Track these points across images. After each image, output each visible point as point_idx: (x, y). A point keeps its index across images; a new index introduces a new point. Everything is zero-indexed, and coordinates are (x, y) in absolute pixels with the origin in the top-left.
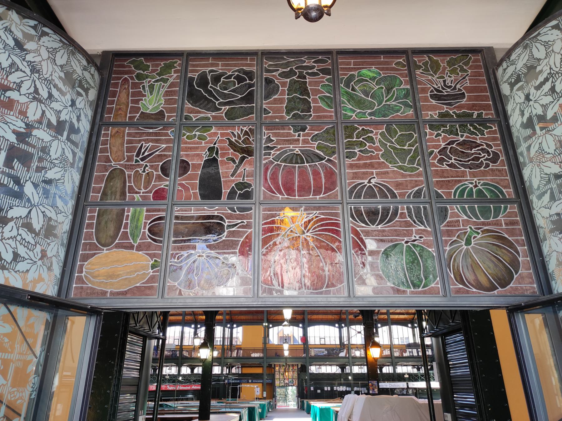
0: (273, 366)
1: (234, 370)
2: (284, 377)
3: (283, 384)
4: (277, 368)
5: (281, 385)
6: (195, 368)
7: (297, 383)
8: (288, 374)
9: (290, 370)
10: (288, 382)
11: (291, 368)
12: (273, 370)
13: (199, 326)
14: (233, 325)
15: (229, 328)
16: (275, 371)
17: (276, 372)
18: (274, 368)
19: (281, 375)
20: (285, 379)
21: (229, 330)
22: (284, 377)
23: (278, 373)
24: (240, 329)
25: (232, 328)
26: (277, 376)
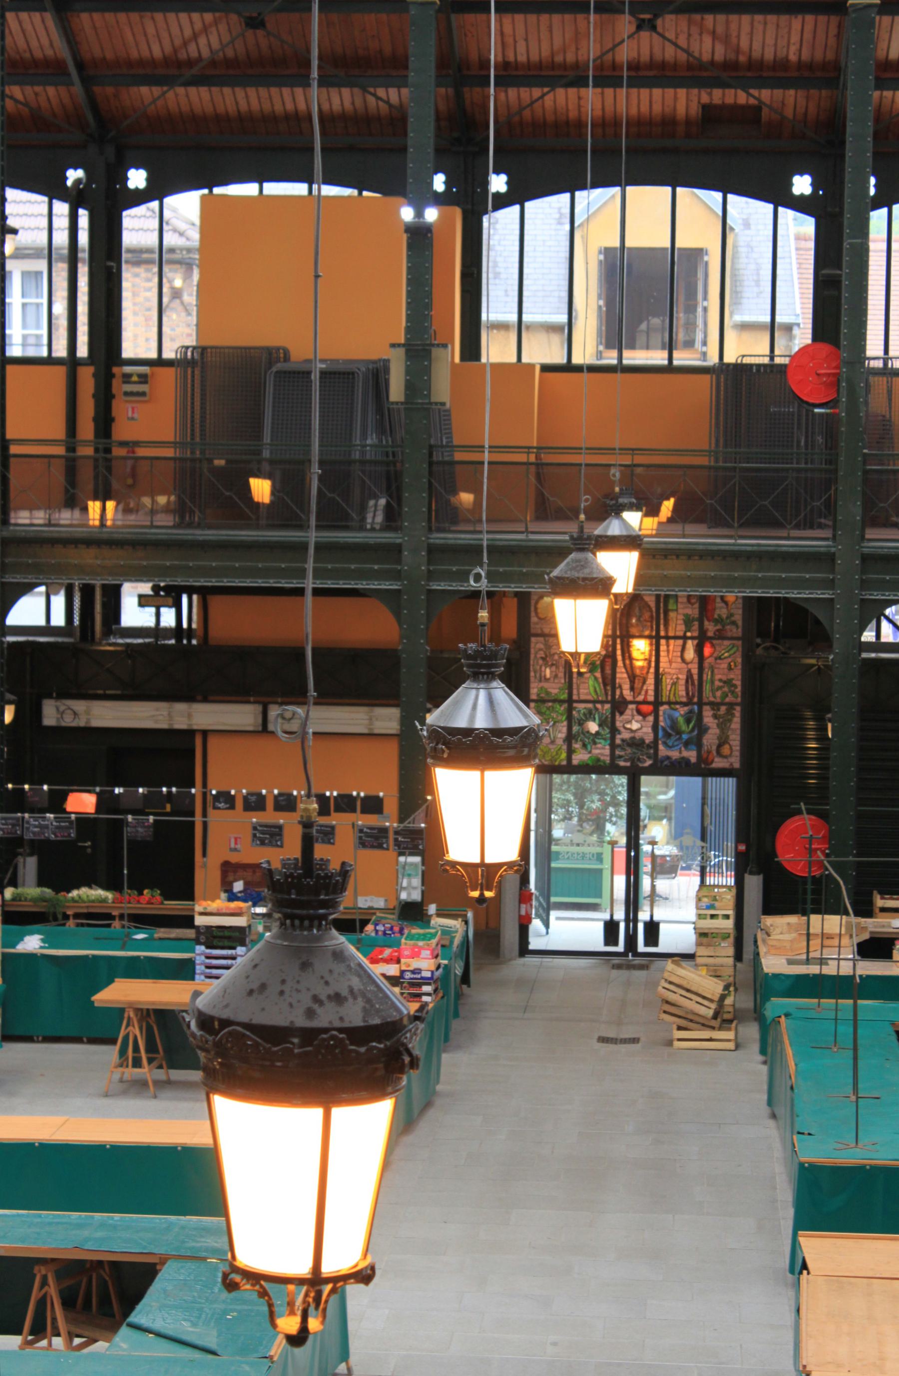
2: (609, 682)
3: (602, 751)
5: (580, 757)
7: (735, 739)
9: (677, 626)
10: (647, 733)
20: (619, 706)
21: (84, 218)
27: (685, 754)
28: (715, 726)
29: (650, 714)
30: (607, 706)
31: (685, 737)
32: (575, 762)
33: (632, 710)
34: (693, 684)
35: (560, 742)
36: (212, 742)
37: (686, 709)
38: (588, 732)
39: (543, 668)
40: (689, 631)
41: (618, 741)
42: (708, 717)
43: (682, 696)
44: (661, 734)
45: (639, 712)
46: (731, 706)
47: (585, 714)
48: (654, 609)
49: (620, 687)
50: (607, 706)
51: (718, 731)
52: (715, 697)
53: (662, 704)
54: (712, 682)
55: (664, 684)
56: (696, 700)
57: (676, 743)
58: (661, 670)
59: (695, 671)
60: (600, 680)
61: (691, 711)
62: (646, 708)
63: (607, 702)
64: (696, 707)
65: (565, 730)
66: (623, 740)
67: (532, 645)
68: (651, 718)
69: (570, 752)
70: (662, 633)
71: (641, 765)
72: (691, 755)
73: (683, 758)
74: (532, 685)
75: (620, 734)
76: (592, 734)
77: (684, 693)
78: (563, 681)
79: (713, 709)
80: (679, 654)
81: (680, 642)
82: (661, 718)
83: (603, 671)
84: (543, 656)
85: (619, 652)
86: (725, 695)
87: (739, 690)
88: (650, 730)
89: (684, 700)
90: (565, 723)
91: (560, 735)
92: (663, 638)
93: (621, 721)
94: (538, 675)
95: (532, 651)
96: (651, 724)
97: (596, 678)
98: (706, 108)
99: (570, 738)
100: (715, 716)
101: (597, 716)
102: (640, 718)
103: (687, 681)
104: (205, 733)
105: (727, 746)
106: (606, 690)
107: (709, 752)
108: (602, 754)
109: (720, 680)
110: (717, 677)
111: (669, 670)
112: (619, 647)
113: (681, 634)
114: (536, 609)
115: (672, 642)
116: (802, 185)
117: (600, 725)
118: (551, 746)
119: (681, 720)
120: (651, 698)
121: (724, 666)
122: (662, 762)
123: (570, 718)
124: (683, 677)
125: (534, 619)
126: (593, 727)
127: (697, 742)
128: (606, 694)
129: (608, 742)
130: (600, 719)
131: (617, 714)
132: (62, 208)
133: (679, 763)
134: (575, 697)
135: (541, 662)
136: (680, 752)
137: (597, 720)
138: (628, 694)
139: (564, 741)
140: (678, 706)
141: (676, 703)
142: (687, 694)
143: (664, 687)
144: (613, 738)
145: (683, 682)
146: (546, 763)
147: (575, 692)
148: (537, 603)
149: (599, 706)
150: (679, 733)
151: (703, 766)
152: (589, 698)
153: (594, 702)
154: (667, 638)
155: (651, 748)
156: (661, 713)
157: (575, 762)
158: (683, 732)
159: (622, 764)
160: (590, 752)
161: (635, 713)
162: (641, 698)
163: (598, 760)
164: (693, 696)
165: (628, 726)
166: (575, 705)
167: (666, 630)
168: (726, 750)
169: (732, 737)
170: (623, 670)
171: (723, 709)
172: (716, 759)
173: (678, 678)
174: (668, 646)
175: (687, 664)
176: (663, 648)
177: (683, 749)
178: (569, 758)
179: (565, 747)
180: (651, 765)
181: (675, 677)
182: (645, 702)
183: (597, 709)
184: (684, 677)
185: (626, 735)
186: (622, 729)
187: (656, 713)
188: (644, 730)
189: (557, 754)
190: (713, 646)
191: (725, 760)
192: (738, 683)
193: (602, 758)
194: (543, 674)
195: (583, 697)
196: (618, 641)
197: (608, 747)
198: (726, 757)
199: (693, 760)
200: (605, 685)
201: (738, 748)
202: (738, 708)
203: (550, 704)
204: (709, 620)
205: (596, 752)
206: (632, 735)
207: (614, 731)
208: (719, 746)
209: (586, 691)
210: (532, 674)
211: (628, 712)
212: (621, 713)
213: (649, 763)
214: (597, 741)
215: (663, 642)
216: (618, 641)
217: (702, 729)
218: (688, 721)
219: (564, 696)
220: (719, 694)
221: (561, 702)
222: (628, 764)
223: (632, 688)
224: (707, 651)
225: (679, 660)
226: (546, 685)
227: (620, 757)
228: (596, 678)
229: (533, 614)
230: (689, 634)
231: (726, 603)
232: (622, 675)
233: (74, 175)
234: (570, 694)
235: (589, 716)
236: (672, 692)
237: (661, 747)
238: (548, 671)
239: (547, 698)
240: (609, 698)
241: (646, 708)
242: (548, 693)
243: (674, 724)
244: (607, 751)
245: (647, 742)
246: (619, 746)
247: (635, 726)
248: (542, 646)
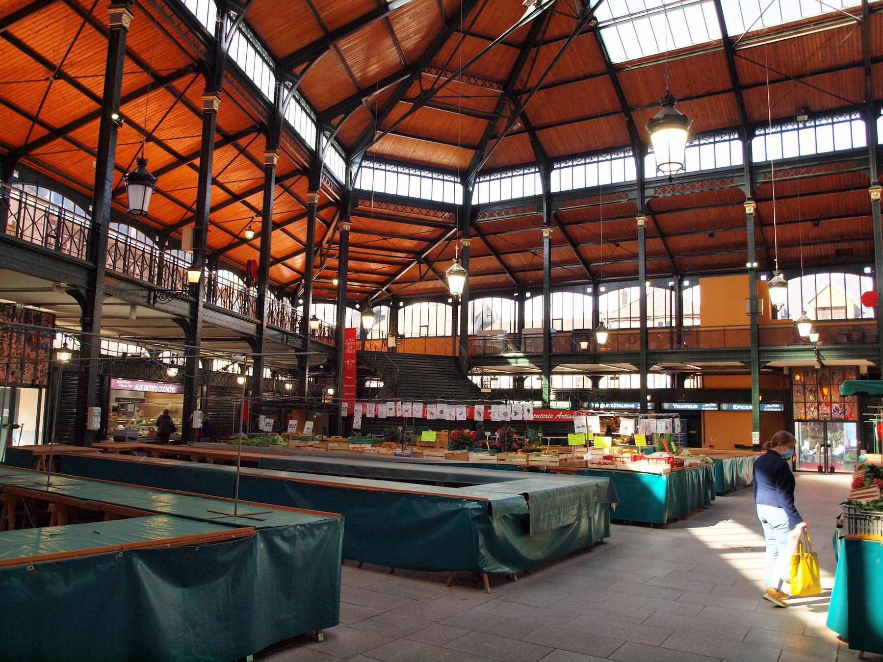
0: (786, 372)
1: (689, 384)
4: (798, 378)
6: (601, 377)
8: (830, 392)
11: (836, 378)
12: (788, 381)
13: (602, 289)
14: (680, 282)
15: (672, 288)
16: (791, 384)
17: (795, 387)
18: (790, 376)
19: (807, 394)
20: (819, 403)
21: (673, 293)
22: (816, 397)
23: (800, 388)
24: (697, 289)
25: (679, 289)
26: (797, 397)
27: (840, 416)
36: (706, 413)
42: (847, 407)
45: (826, 405)
46: (854, 403)
62: (827, 404)
68: (829, 407)
69: (806, 416)
72: (842, 416)
86: (851, 400)
98: (837, 251)
99: (805, 412)
100: (849, 406)
104: (704, 411)
116: (867, 270)
120: (829, 401)
123: (805, 407)
125: (793, 380)
126: (812, 409)
127: (844, 413)
132: (668, 291)
138: (822, 400)
150: (838, 410)
154: (833, 384)
168: (853, 415)
171: (851, 404)
176: (832, 387)
178: (806, 418)
182: (827, 402)
185: (822, 411)
187: (831, 405)
202: (856, 404)
207: (818, 410)
208: (851, 414)
217: (845, 410)
218: (841, 407)
232: (820, 395)
233: (671, 284)
235: (811, 406)
241: (827, 404)
243: (836, 407)
247: (825, 409)
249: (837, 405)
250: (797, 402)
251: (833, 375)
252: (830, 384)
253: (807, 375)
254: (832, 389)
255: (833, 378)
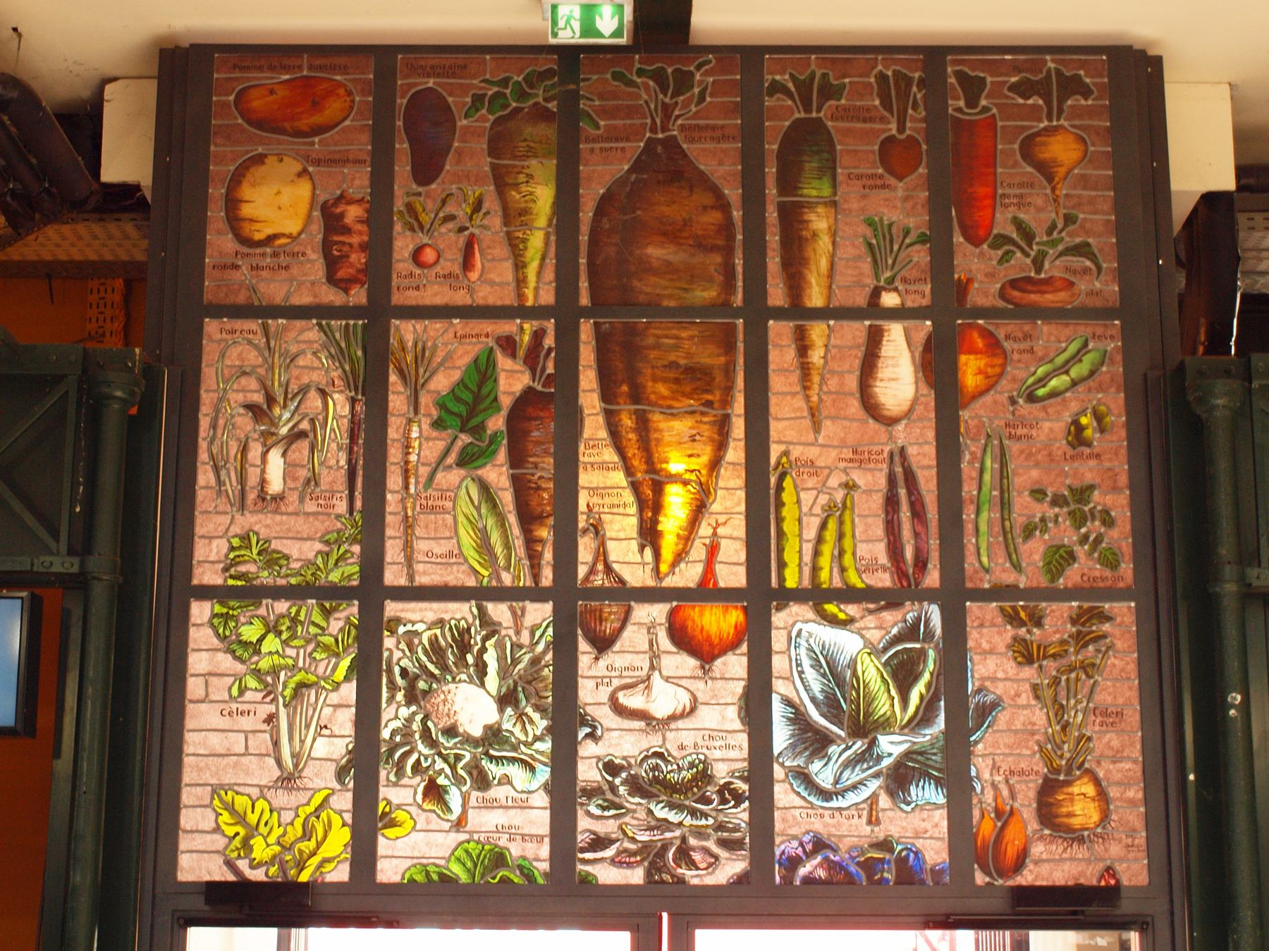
28: (1026, 698)
29: (733, 646)
30: (540, 612)
31: (891, 746)
32: (389, 871)
33: (651, 628)
34: (918, 513)
35: (320, 777)
37: (893, 621)
38: (451, 731)
39: (255, 451)
40: (890, 285)
41: (588, 773)
43: (871, 567)
44: (781, 736)
45: (682, 637)
47: (435, 650)
48: (733, 194)
49: (597, 529)
50: (540, 612)
51: (1039, 716)
52: (1017, 567)
53: (786, 597)
54: (1004, 504)
55: (789, 512)
56: (933, 578)
57: (851, 777)
58: (775, 451)
59: (924, 456)
60: (507, 498)
61: (911, 632)
63: (537, 594)
64: (934, 613)
65: (345, 722)
66: (612, 768)
67: (210, 351)
68: (735, 665)
70: (777, 295)
71: (693, 877)
73: (885, 845)
74: (203, 525)
75: (592, 736)
76: (468, 740)
77: (880, 551)
78: (342, 507)
79: (1013, 618)
80: (852, 382)
81: (856, 331)
82: (779, 663)
83: (517, 459)
84: (258, 398)
85: (588, 379)
86: (1060, 558)
87: (1121, 536)
88: (731, 718)
89: (884, 580)
90: (349, 691)
91: (322, 748)
92: (779, 314)
93: (599, 681)
94: (231, 485)
95: (209, 376)
96: (739, 687)
97: (484, 487)
100: (1026, 654)
101: (491, 658)
102: (688, 663)
103: (891, 502)
105: (1084, 788)
106: (531, 542)
107: (1004, 816)
108: (512, 832)
109: (1038, 493)
110: (1024, 476)
111: (813, 452)
112: (587, 355)
113: (861, 300)
114: (232, 203)
115: (817, 331)
117: (506, 700)
118: (281, 798)
119: (872, 672)
120: (732, 575)
121: (1052, 427)
122: (793, 863)
124: (873, 480)
125: (220, 243)
128: (534, 558)
129: (544, 774)
130: (503, 673)
131: (583, 645)
133: (870, 866)
134: (393, 576)
135: (245, 422)
136: (873, 821)
137: (492, 680)
139: (341, 774)
140: (852, 610)
141: (848, 594)
142: (895, 550)
143: (789, 527)
144: (564, 760)
145: (870, 506)
146: (258, 875)
147: (393, 551)
148: (237, 179)
149: (499, 611)
151: (980, 878)
152: (457, 577)
153: (480, 594)
155: (738, 798)
156: (778, 640)
157: (389, 871)
158: (885, 725)
159: (607, 875)
160: (459, 824)
161: (665, 642)
162: (688, 575)
163: (499, 859)
164: (921, 563)
165: (631, 700)
166: (392, 608)
167: (795, 284)
169: (1105, 740)
170: (610, 455)
172: (1038, 849)
173: (849, 487)
174: (803, 349)
175: (891, 421)
176: (781, 355)
177: (884, 801)
179: (344, 801)
180: (741, 880)
181: (834, 482)
182: (707, 591)
183: (490, 627)
184: (882, 481)
186: (605, 716)
188: (707, 717)
189: (307, 834)
190: (994, 346)
191: (1080, 852)
192: (1119, 503)
193: (515, 850)
194: (253, 479)
195: (427, 576)
196: (586, 330)
197: (542, 799)
198: (1075, 836)
199: (935, 853)
200: (528, 518)
201: (1136, 793)
202: (1124, 612)
203: (282, 606)
204: (975, 241)
205: (484, 821)
206: (653, 741)
208: (1049, 790)
209: (440, 548)
210: (205, 477)
211: (633, 637)
212: (602, 644)
213: (732, 867)
214: (494, 770)
215: (780, 331)
216: (586, 330)
219: (347, 572)
220: (1034, 551)
221: (331, 595)
222: (636, 876)
223: (649, 534)
224: (971, 369)
225: (854, 406)
226: (261, 523)
227: (599, 843)
228: (484, 487)
229: (216, 214)
230: (890, 300)
231: (1046, 170)
234: (373, 564)
236: (827, 550)
237: (784, 794)
238: (275, 462)
239: (265, 578)
240: (547, 578)
242: (272, 559)
244: (539, 820)
245: (721, 772)
246: (592, 792)
247: (664, 701)
248: (253, 358)
249: (846, 644)
250: (252, 594)
251: (788, 183)
252: (758, 313)
253: (426, 171)
254: (781, 382)
255: (792, 218)
